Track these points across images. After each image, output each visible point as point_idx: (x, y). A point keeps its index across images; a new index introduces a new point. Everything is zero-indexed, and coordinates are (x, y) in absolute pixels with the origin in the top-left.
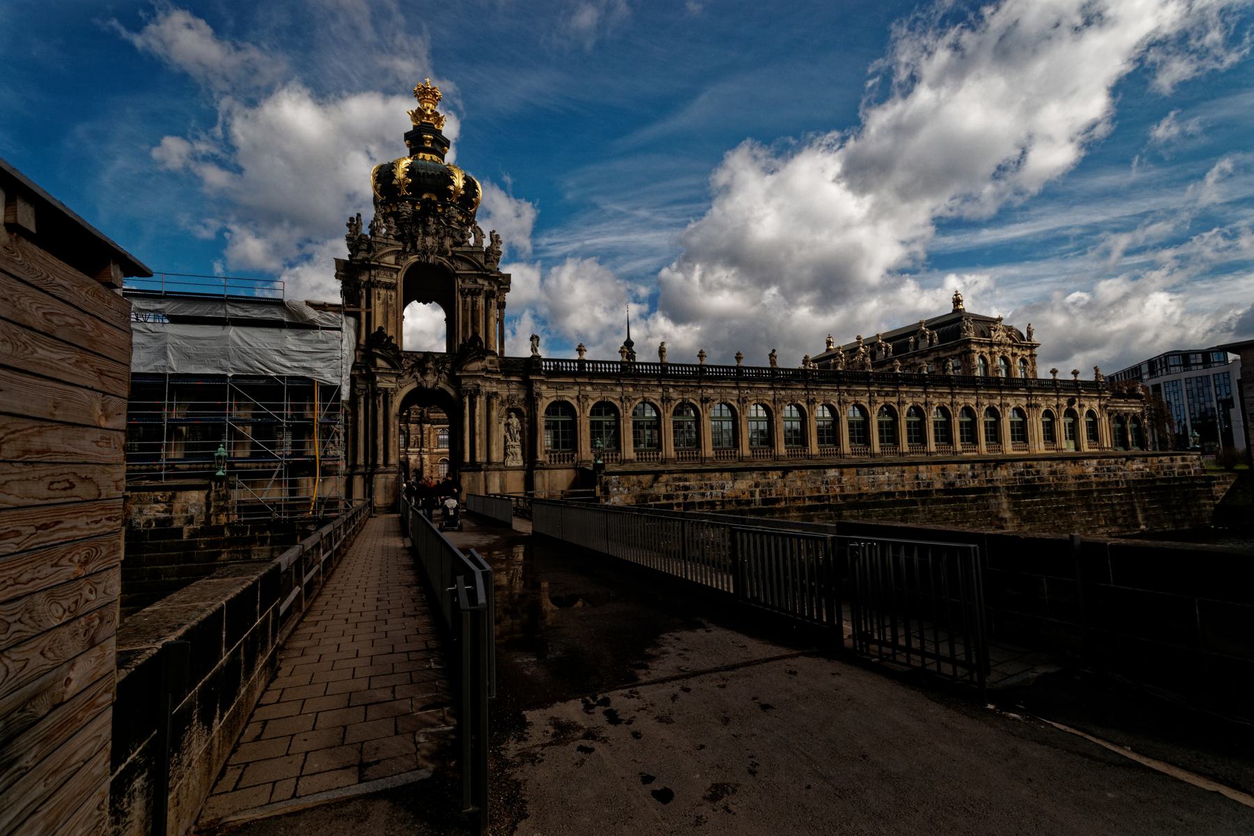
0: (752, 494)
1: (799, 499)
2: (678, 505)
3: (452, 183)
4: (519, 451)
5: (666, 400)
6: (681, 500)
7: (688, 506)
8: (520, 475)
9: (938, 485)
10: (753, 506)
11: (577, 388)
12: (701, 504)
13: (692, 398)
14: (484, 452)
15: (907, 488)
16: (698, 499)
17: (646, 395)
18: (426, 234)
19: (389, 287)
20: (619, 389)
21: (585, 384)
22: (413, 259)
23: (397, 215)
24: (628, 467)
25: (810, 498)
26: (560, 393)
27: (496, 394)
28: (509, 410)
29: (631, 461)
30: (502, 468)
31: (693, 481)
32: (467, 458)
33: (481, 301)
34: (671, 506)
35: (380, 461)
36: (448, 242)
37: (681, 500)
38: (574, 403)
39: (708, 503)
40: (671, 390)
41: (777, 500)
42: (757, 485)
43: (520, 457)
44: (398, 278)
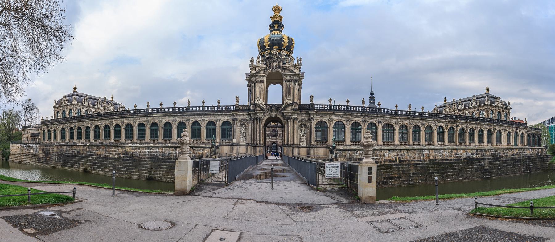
4: (305, 140)
5: (364, 121)
8: (305, 149)
9: (464, 157)
11: (328, 116)
13: (374, 121)
14: (292, 141)
15: (453, 158)
17: (356, 119)
18: (274, 61)
19: (261, 82)
20: (345, 116)
21: (331, 114)
22: (269, 71)
23: (264, 56)
24: (347, 148)
26: (321, 118)
27: (297, 119)
28: (302, 125)
29: (349, 145)
30: (299, 147)
32: (286, 143)
33: (292, 84)
35: (258, 143)
36: (281, 64)
38: (327, 122)
40: (366, 118)
43: (305, 143)
44: (265, 79)
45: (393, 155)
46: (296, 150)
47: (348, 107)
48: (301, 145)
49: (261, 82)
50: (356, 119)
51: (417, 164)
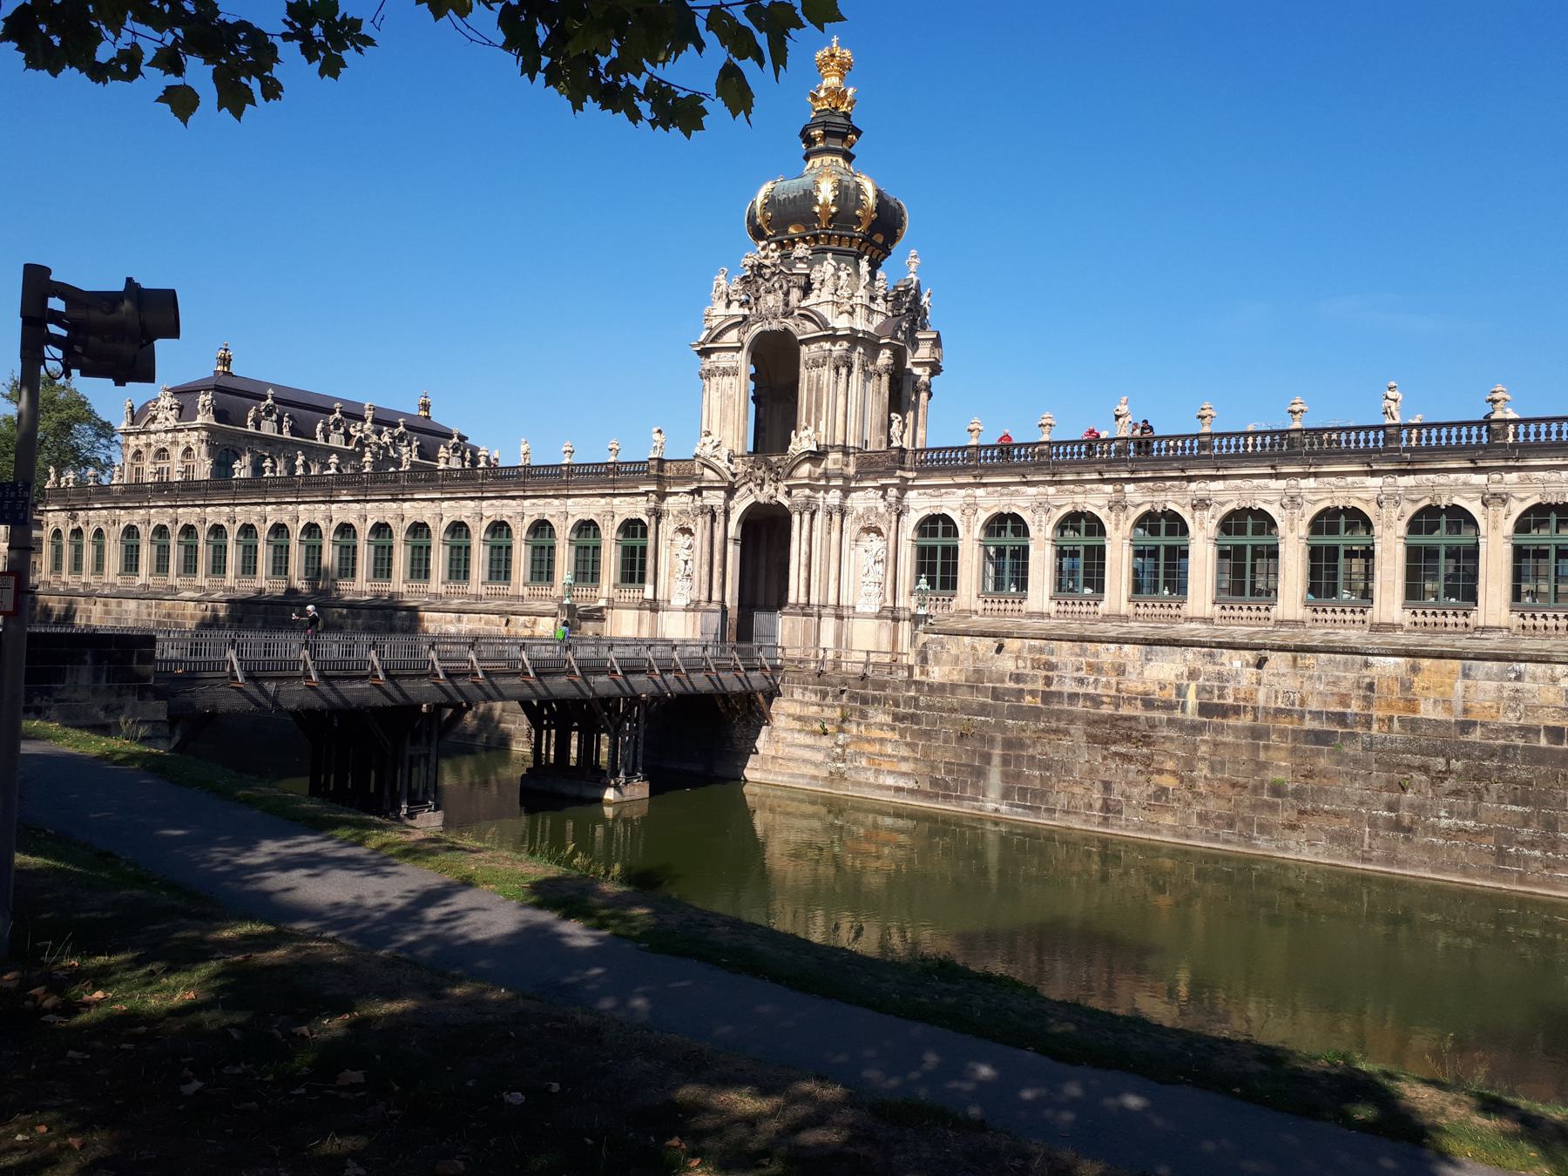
0: (1181, 692)
1: (1289, 713)
2: (1033, 693)
6: (1040, 686)
7: (1047, 697)
10: (1178, 714)
12: (1073, 697)
16: (1069, 687)
25: (1317, 715)
26: (936, 502)
31: (1064, 653)
34: (1020, 694)
39: (1086, 696)
41: (1236, 710)
42: (1193, 675)
45: (1165, 669)
50: (1079, 499)
51: (1320, 738)
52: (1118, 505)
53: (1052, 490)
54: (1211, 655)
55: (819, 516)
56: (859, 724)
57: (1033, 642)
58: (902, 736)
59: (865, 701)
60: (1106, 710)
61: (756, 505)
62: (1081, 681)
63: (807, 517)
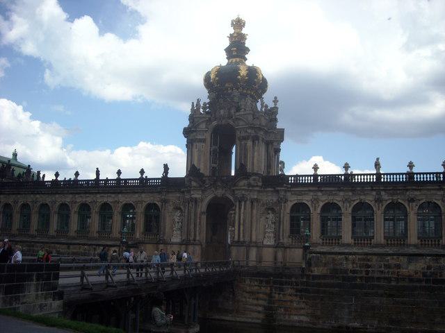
3: (239, 74)
4: (272, 235)
6: (364, 274)
12: (379, 279)
16: (376, 275)
17: (362, 197)
20: (342, 193)
22: (215, 123)
26: (300, 198)
27: (257, 200)
29: (348, 245)
30: (259, 246)
37: (364, 274)
38: (309, 204)
39: (385, 278)
40: (383, 193)
46: (253, 253)
47: (315, 176)
48: (265, 243)
49: (203, 141)
50: (362, 197)
52: (379, 200)
53: (350, 194)
54: (437, 260)
55: (248, 202)
56: (279, 294)
57: (360, 257)
58: (301, 298)
59: (281, 284)
60: (393, 283)
61: (215, 198)
62: (382, 272)
63: (243, 203)
